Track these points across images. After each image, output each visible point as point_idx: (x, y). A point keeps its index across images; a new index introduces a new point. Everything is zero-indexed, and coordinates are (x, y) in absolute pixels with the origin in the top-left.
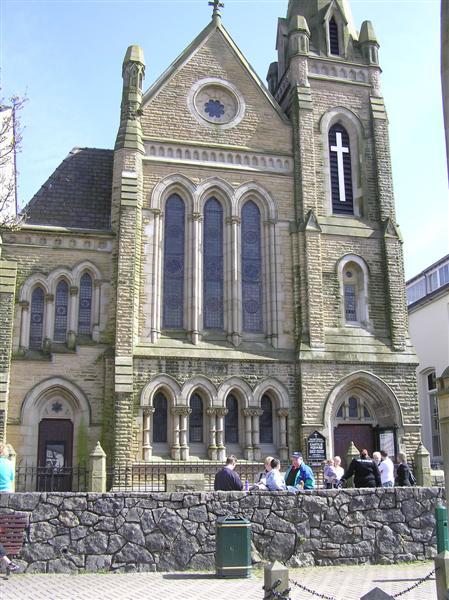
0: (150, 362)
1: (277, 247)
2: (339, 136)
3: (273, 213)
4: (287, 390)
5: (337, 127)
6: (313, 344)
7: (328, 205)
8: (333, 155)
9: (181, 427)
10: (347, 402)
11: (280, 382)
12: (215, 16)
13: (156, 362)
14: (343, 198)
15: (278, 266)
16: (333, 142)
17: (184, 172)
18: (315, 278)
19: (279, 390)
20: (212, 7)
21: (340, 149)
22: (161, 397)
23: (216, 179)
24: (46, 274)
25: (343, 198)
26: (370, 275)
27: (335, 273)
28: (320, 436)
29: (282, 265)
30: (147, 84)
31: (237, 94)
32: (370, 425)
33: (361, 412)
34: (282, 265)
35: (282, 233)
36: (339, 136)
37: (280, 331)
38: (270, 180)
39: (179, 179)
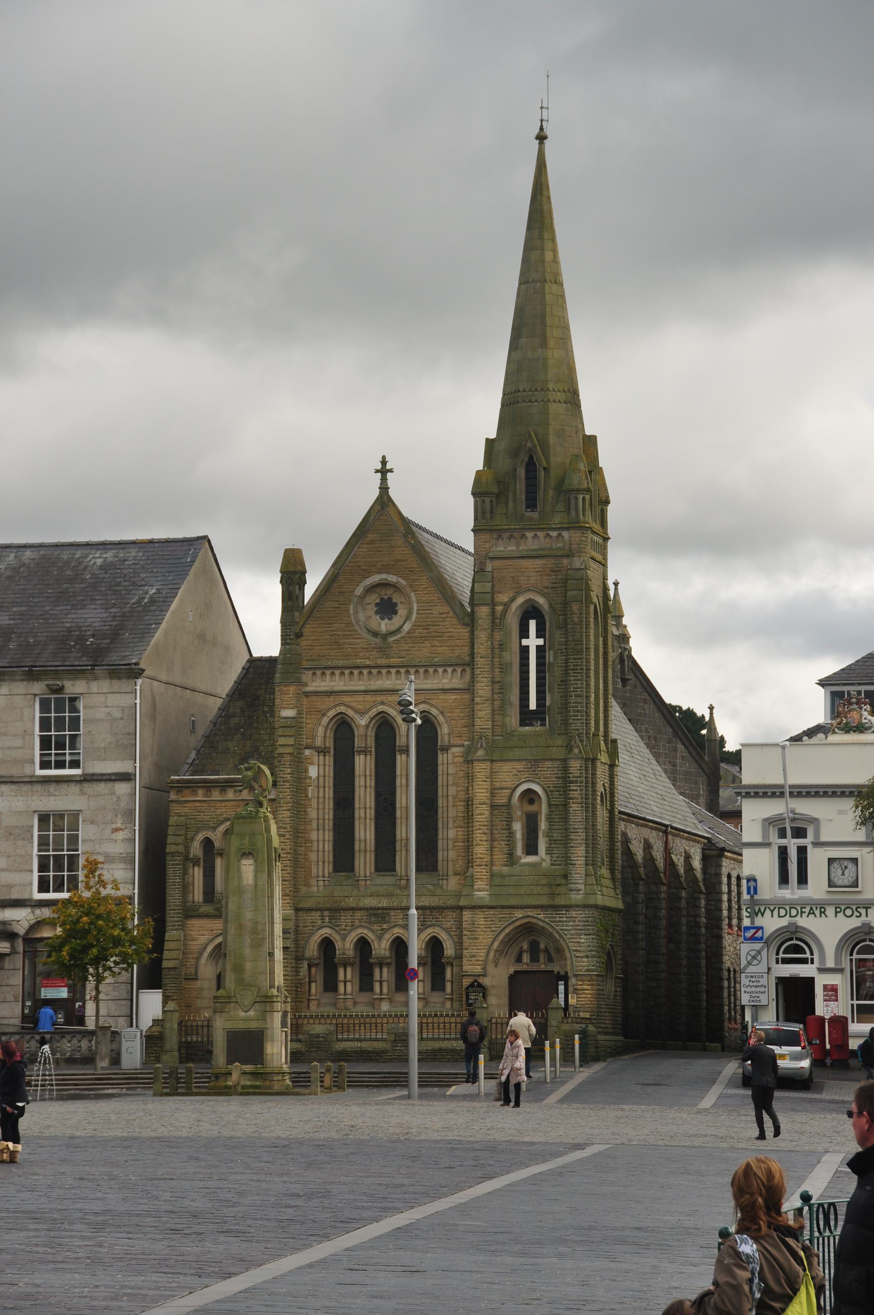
0: (313, 913)
1: (450, 778)
2: (533, 624)
3: (446, 737)
4: (451, 936)
5: (531, 612)
6: (476, 887)
7: (513, 718)
8: (525, 650)
9: (347, 977)
10: (525, 946)
11: (445, 930)
12: (384, 488)
13: (319, 913)
14: (533, 705)
15: (450, 799)
16: (524, 634)
17: (346, 699)
18: (482, 814)
19: (443, 936)
20: (379, 475)
21: (533, 642)
22: (327, 945)
23: (382, 703)
24: (214, 829)
25: (533, 705)
26: (550, 805)
27: (508, 805)
28: (480, 985)
29: (454, 797)
30: (310, 591)
31: (409, 590)
32: (552, 972)
33: (542, 957)
34: (454, 797)
35: (456, 759)
36: (533, 624)
37: (450, 872)
38: (443, 697)
39: (343, 709)
